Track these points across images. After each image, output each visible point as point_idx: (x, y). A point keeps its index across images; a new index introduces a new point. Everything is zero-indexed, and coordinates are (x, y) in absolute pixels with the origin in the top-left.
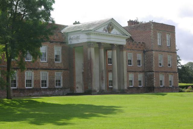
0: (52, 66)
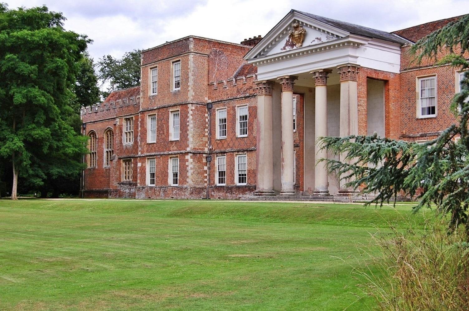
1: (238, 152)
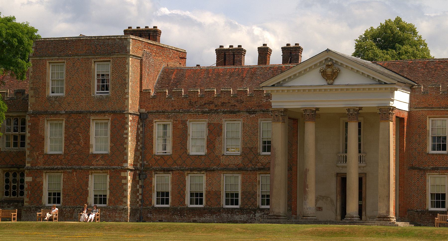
0: (251, 162)
1: (191, 170)
